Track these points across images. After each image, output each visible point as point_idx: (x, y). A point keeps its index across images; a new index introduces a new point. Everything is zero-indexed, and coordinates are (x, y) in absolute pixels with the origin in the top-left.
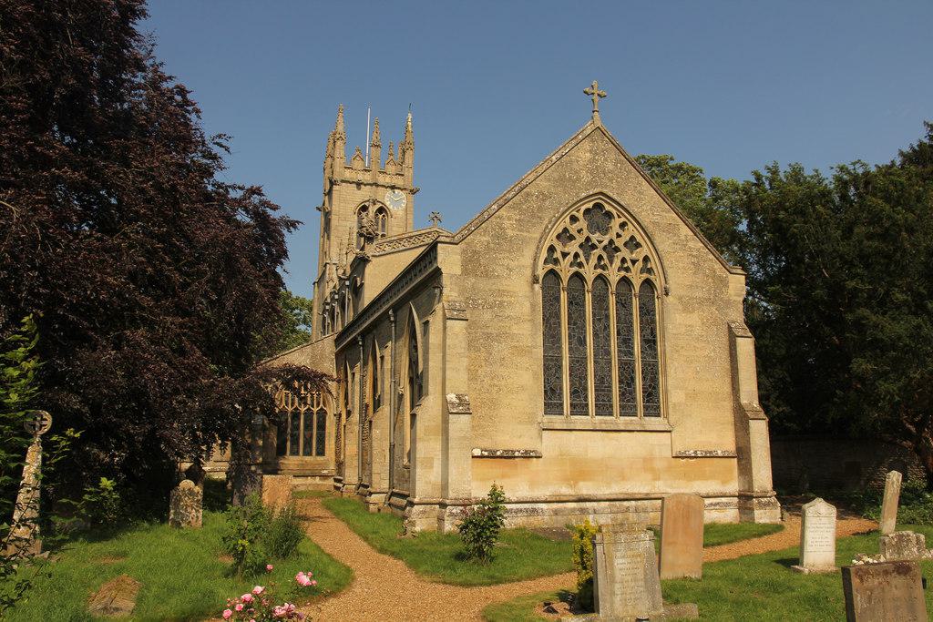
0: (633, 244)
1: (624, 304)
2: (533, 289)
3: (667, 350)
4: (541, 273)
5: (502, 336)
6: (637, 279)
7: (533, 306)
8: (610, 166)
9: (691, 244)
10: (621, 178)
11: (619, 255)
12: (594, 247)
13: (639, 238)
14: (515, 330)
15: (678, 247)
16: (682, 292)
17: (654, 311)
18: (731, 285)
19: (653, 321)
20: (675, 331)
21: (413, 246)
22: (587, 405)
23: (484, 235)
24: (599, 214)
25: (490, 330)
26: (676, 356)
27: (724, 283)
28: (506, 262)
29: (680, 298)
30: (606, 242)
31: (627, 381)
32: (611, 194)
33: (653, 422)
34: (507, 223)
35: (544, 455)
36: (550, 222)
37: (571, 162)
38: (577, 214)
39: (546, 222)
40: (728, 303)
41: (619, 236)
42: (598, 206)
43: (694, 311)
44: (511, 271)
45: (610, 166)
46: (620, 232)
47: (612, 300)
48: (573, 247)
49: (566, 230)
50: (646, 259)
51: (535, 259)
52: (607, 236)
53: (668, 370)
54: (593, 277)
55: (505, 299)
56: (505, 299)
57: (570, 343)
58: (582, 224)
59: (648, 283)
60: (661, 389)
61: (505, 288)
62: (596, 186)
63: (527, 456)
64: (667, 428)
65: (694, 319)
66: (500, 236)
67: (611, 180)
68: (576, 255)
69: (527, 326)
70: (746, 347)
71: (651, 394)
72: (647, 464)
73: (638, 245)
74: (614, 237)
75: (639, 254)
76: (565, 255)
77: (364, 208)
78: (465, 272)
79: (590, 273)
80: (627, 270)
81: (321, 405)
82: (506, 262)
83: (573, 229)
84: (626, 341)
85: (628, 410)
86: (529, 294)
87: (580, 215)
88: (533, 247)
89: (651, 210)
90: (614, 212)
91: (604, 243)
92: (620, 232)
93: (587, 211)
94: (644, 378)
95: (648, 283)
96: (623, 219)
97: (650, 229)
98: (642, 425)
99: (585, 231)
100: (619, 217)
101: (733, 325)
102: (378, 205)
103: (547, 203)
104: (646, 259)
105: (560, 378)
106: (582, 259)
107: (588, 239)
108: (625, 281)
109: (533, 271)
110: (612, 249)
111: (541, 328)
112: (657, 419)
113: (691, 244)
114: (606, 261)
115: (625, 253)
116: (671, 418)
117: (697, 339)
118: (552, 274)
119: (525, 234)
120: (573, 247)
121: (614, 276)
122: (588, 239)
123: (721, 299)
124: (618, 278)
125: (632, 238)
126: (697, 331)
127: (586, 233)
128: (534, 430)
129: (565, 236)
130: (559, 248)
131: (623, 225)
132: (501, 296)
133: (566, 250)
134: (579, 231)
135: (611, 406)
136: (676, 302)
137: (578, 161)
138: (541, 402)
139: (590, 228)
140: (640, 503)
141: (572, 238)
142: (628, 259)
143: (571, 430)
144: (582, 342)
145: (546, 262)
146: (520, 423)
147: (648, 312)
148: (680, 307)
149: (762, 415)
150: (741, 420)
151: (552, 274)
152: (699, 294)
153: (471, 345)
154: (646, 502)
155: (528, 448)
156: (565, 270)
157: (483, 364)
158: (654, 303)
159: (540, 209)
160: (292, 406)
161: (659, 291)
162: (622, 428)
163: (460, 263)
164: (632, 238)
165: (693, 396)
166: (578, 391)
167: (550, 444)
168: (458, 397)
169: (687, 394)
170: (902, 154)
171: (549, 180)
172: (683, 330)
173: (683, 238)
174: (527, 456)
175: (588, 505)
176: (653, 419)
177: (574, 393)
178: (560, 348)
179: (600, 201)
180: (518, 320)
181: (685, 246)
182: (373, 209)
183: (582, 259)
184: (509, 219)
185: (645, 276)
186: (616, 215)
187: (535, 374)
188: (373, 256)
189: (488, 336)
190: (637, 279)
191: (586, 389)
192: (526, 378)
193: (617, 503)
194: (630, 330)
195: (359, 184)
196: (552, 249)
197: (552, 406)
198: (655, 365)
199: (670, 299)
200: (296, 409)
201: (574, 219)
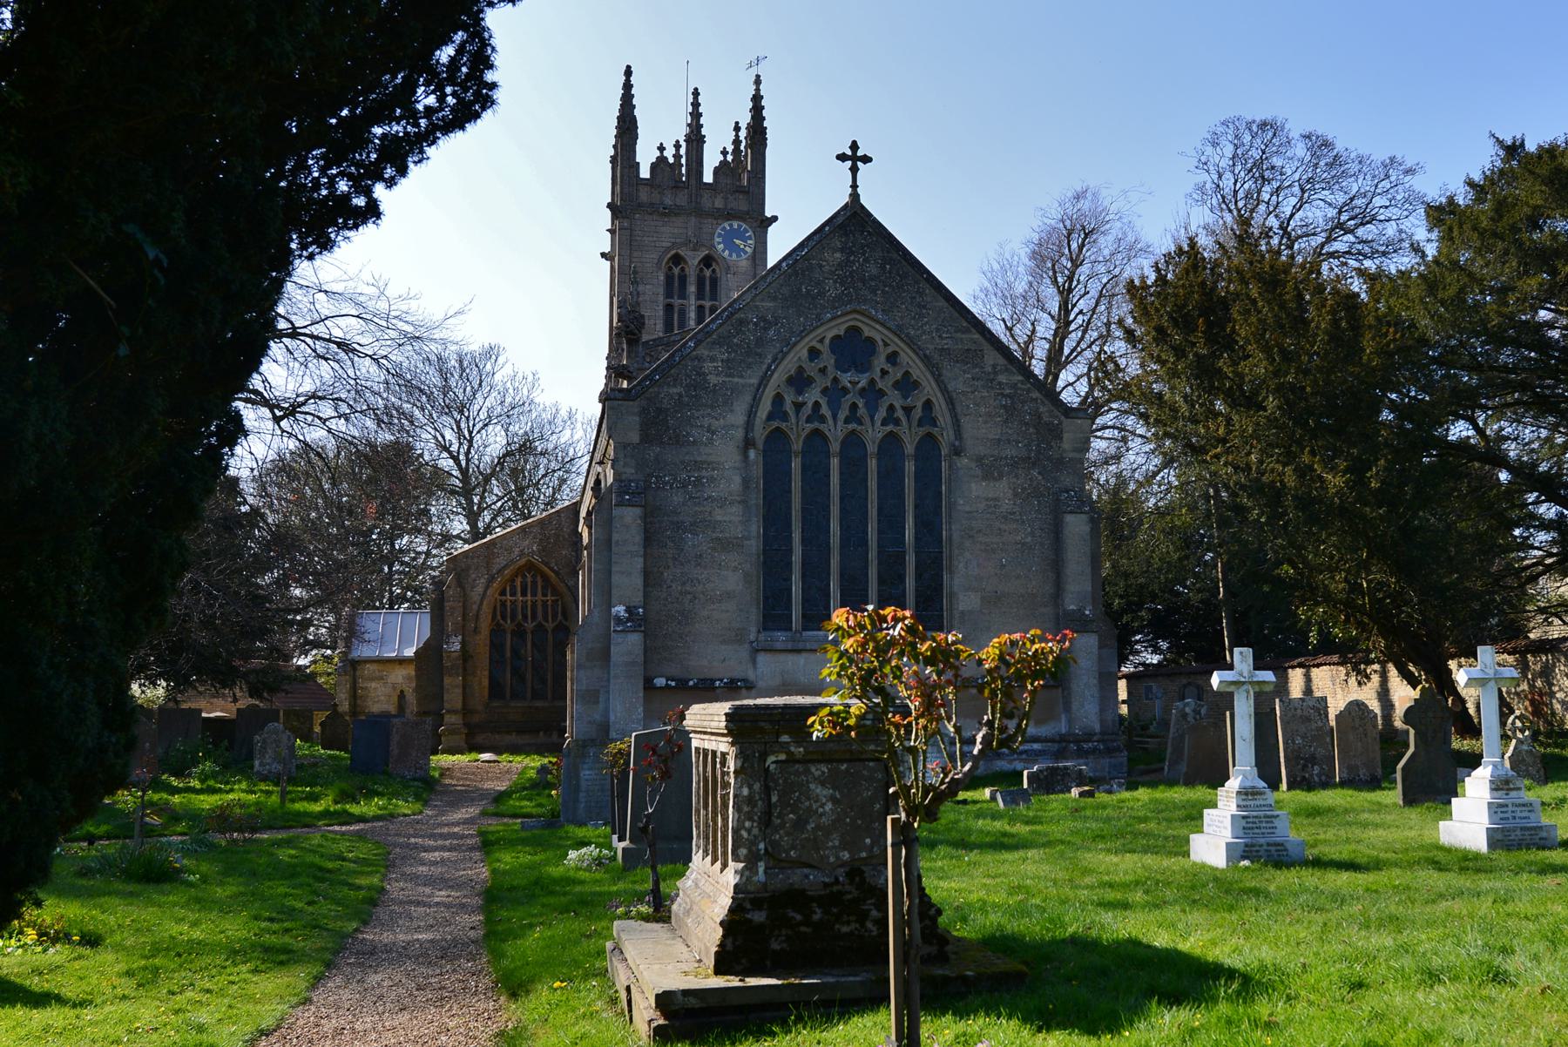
2: (746, 457)
4: (760, 434)
7: (746, 482)
8: (873, 269)
9: (1002, 378)
10: (890, 286)
14: (719, 516)
15: (979, 383)
18: (1066, 436)
20: (967, 508)
23: (675, 386)
26: (968, 543)
28: (706, 421)
29: (979, 460)
30: (863, 383)
34: (708, 366)
36: (773, 361)
38: (818, 346)
39: (769, 360)
41: (884, 373)
42: (854, 331)
43: (1001, 476)
44: (713, 433)
46: (888, 367)
48: (812, 396)
49: (800, 369)
50: (928, 405)
51: (751, 414)
53: (956, 563)
54: (841, 435)
55: (704, 473)
56: (704, 473)
58: (828, 359)
60: (945, 592)
61: (711, 459)
62: (850, 302)
65: (1002, 489)
67: (874, 292)
68: (817, 405)
73: (916, 385)
78: (646, 439)
79: (836, 432)
81: (560, 617)
83: (811, 369)
87: (824, 348)
88: (748, 398)
89: (937, 330)
90: (878, 338)
91: (860, 385)
93: (836, 338)
95: (928, 444)
96: (890, 350)
99: (830, 369)
100: (886, 345)
106: (825, 410)
107: (835, 380)
109: (747, 433)
113: (1002, 378)
115: (895, 398)
117: (1005, 518)
119: (736, 380)
121: (873, 434)
122: (835, 380)
124: (880, 435)
126: (1006, 505)
128: (744, 652)
129: (799, 381)
130: (789, 399)
132: (700, 469)
134: (823, 371)
136: (973, 465)
137: (821, 266)
138: (755, 615)
139: (838, 367)
142: (897, 405)
143: (799, 651)
146: (724, 642)
147: (929, 479)
148: (979, 472)
152: (1010, 452)
153: (649, 539)
155: (737, 674)
157: (671, 564)
159: (760, 342)
160: (512, 620)
163: (638, 426)
168: (628, 610)
169: (983, 598)
170: (1471, 183)
171: (775, 299)
172: (982, 506)
179: (852, 323)
180: (723, 502)
181: (992, 381)
182: (693, 260)
183: (825, 410)
184: (713, 359)
186: (880, 343)
188: (638, 369)
196: (778, 399)
199: (964, 461)
200: (519, 625)
201: (814, 353)
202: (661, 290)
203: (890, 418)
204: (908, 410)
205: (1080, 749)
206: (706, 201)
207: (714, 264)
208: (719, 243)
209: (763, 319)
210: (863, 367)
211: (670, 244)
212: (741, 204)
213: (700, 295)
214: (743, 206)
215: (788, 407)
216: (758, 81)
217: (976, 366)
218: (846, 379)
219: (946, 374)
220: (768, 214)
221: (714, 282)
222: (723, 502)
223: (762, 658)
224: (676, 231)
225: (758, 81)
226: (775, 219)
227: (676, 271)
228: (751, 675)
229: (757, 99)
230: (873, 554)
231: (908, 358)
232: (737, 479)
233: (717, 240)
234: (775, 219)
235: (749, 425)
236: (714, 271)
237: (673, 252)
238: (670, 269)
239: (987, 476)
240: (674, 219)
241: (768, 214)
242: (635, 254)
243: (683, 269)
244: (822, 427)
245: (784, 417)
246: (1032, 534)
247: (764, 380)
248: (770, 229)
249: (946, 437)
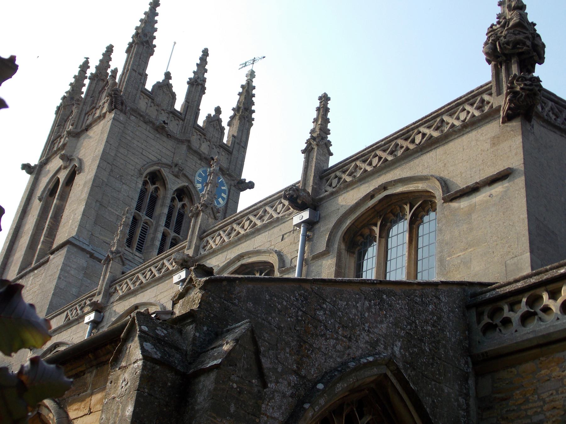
102: (181, 183)
182: (174, 184)
206: (195, 139)
207: (186, 201)
208: (199, 182)
211: (155, 159)
212: (220, 158)
213: (167, 225)
216: (252, 75)
220: (247, 175)
224: (164, 150)
225: (252, 75)
227: (151, 188)
233: (198, 178)
236: (184, 206)
237: (156, 168)
240: (165, 139)
243: (157, 189)
248: (242, 193)
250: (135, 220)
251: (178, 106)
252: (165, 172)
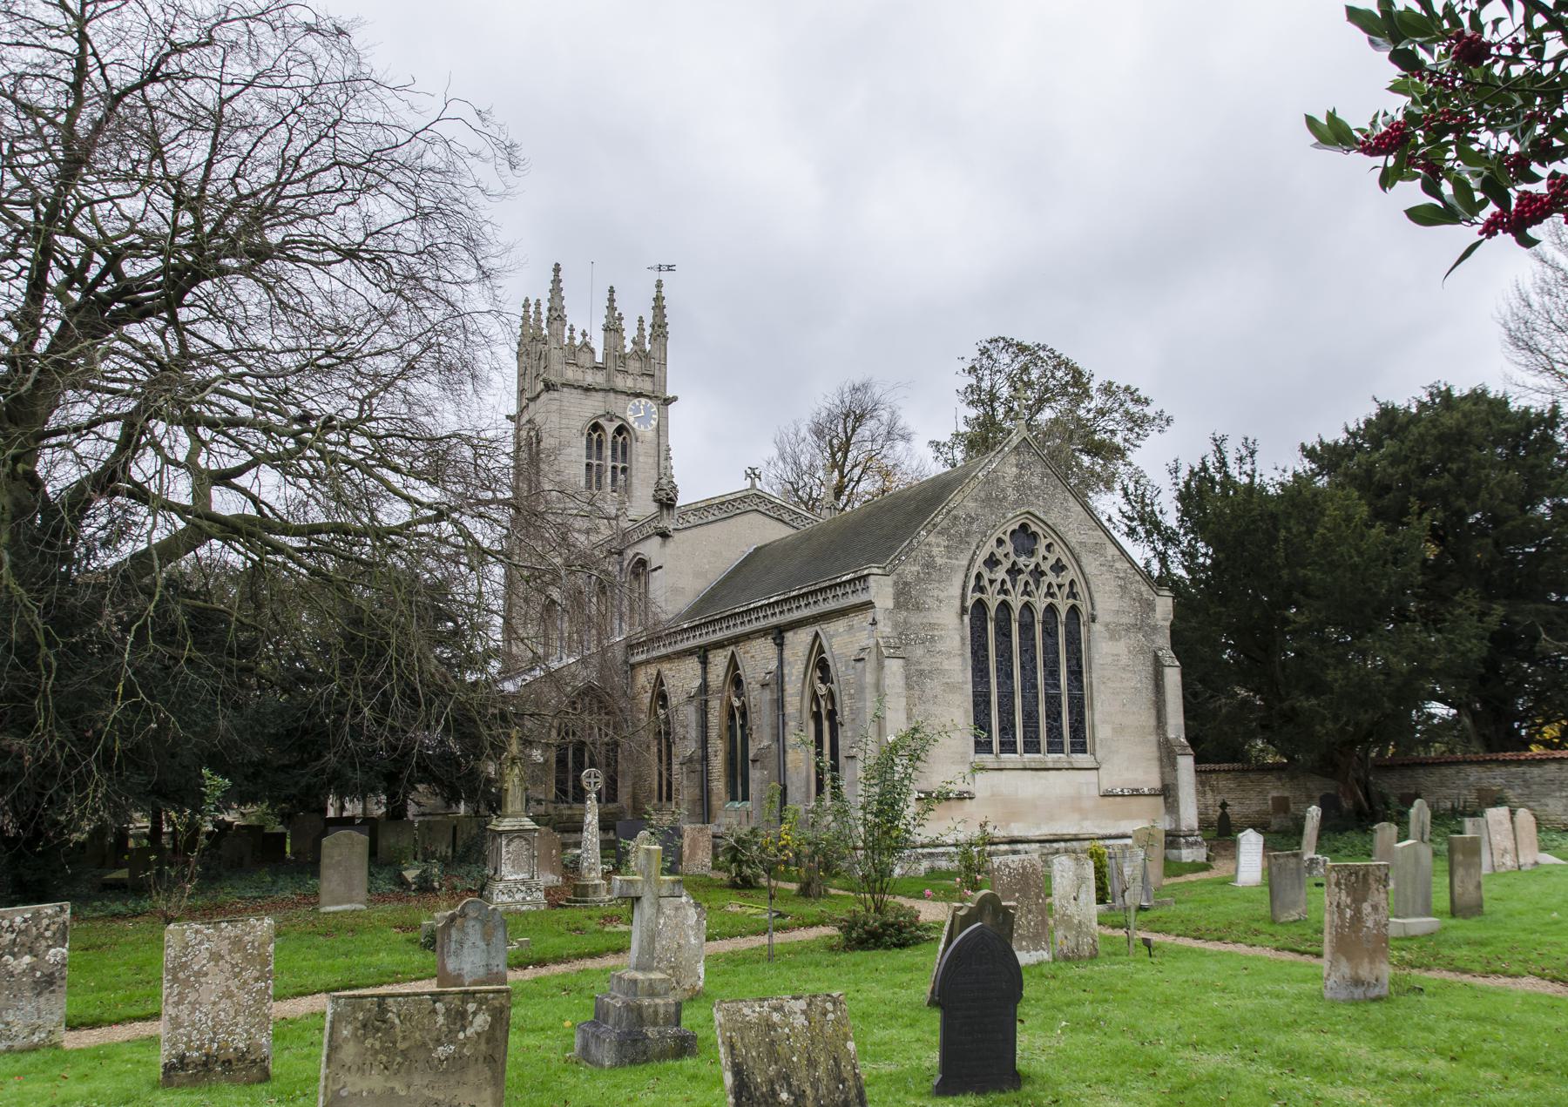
0: (1059, 568)
1: (1050, 633)
2: (962, 620)
3: (1094, 684)
4: (969, 603)
5: (934, 672)
6: (1063, 607)
7: (963, 639)
8: (1036, 481)
9: (1118, 565)
11: (1045, 580)
12: (1020, 571)
13: (1065, 561)
14: (946, 665)
15: (1104, 568)
16: (1108, 619)
17: (1080, 639)
18: (1157, 609)
19: (1080, 651)
21: (725, 515)
22: (1015, 742)
24: (1025, 537)
25: (922, 667)
26: (1102, 687)
27: (1150, 606)
29: (1107, 625)
30: (1032, 567)
31: (1054, 716)
32: (1037, 513)
33: (1081, 759)
34: (935, 551)
35: (978, 795)
37: (997, 477)
38: (1003, 537)
39: (974, 547)
40: (1155, 629)
41: (1045, 558)
42: (1024, 527)
45: (1036, 481)
46: (1046, 554)
47: (1038, 628)
48: (1000, 574)
50: (1072, 583)
51: (964, 588)
52: (1033, 560)
54: (1020, 605)
55: (936, 633)
56: (936, 633)
57: (998, 677)
58: (1009, 547)
59: (1074, 611)
63: (961, 797)
64: (1094, 765)
66: (929, 565)
67: (1037, 497)
68: (1003, 582)
69: (958, 661)
70: (1173, 677)
71: (1078, 728)
72: (1075, 804)
73: (1063, 568)
74: (1041, 561)
75: (1065, 578)
76: (992, 582)
77: (596, 427)
78: (898, 606)
79: (1017, 601)
80: (1052, 595)
82: (936, 593)
83: (999, 555)
84: (1052, 673)
85: (1056, 747)
86: (958, 626)
87: (1007, 538)
88: (962, 576)
90: (1040, 532)
92: (1046, 554)
93: (1013, 532)
94: (1070, 712)
95: (1074, 611)
96: (1049, 541)
97: (1077, 549)
98: (1070, 763)
101: (1160, 653)
102: (618, 423)
103: (975, 526)
104: (1072, 583)
105: (989, 715)
106: (1009, 585)
108: (1051, 609)
110: (1038, 573)
111: (970, 662)
112: (1084, 755)
113: (1118, 565)
114: (1032, 587)
115: (1051, 577)
116: (1099, 755)
118: (980, 604)
119: (954, 561)
120: (1000, 574)
121: (1040, 603)
122: (1014, 563)
123: (1148, 625)
124: (1044, 606)
125: (1059, 560)
126: (1124, 660)
127: (1012, 557)
129: (992, 562)
130: (986, 575)
131: (1049, 547)
133: (993, 576)
134: (1006, 555)
135: (1039, 743)
136: (1103, 629)
139: (1016, 551)
140: (1069, 844)
141: (998, 563)
144: (1010, 676)
145: (973, 591)
148: (1107, 635)
149: (1190, 750)
150: (1167, 754)
151: (980, 604)
152: (1125, 620)
154: (1074, 843)
156: (993, 601)
158: (1079, 632)
159: (968, 533)
161: (1084, 618)
162: (1051, 766)
164: (1059, 560)
165: (1120, 730)
166: (1007, 728)
167: (983, 784)
172: (1109, 660)
173: (1110, 558)
174: (961, 797)
175: (1020, 847)
176: (1080, 755)
177: (1002, 730)
178: (988, 682)
180: (949, 655)
182: (610, 428)
183: (1009, 585)
184: (938, 546)
185: (1071, 601)
187: (966, 711)
189: (921, 673)
190: (1063, 607)
191: (1014, 726)
192: (955, 712)
193: (1047, 845)
194: (1056, 662)
195: (587, 389)
196: (979, 576)
197: (982, 746)
198: (1081, 698)
199: (1096, 627)
201: (1000, 542)
202: (584, 452)
203: (1051, 594)
204: (1060, 587)
205: (1187, 842)
207: (625, 434)
209: (968, 515)
210: (1032, 553)
212: (646, 385)
213: (614, 458)
214: (646, 385)
215: (985, 582)
216: (659, 285)
217: (1102, 555)
218: (1022, 561)
219: (1084, 561)
221: (624, 447)
222: (949, 655)
223: (979, 776)
225: (659, 285)
226: (675, 399)
227: (595, 436)
228: (971, 788)
229: (659, 299)
230: (1042, 696)
231: (1059, 552)
232: (958, 638)
234: (675, 399)
235: (964, 597)
238: (589, 435)
239: (1112, 638)
241: (669, 394)
242: (563, 421)
244: (1008, 598)
245: (982, 589)
246: (1141, 681)
247: (972, 561)
249: (1084, 609)
250: (589, 466)
251: (599, 358)
252: (602, 421)
